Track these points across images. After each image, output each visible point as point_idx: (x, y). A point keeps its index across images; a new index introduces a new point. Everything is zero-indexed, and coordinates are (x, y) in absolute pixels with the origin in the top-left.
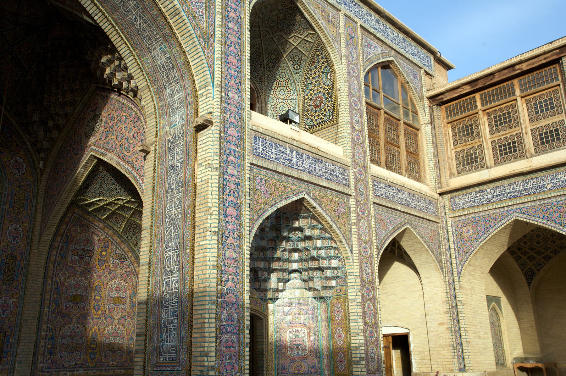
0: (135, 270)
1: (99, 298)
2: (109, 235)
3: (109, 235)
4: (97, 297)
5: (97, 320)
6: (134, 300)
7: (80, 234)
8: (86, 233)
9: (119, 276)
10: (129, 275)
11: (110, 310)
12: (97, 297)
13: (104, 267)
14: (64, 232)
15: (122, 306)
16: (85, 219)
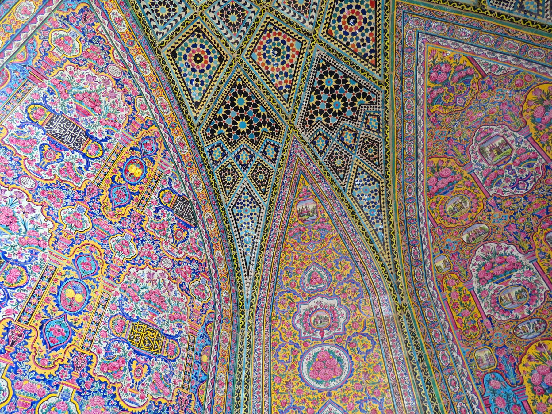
0: (214, 266)
1: (79, 298)
2: (162, 119)
3: (162, 119)
4: (69, 293)
5: (40, 386)
6: (205, 358)
7: (77, 63)
8: (99, 71)
9: (167, 263)
10: (196, 272)
11: (112, 366)
12: (69, 293)
13: (125, 211)
14: (26, 28)
15: (157, 364)
16: (107, 17)
